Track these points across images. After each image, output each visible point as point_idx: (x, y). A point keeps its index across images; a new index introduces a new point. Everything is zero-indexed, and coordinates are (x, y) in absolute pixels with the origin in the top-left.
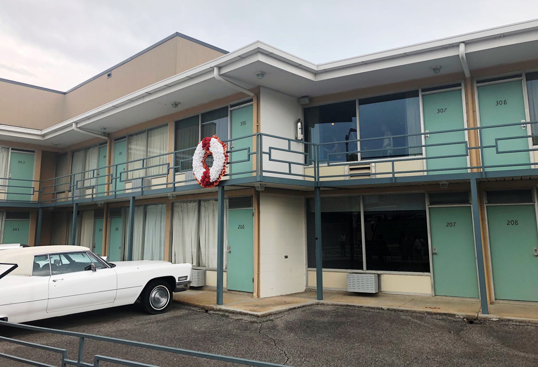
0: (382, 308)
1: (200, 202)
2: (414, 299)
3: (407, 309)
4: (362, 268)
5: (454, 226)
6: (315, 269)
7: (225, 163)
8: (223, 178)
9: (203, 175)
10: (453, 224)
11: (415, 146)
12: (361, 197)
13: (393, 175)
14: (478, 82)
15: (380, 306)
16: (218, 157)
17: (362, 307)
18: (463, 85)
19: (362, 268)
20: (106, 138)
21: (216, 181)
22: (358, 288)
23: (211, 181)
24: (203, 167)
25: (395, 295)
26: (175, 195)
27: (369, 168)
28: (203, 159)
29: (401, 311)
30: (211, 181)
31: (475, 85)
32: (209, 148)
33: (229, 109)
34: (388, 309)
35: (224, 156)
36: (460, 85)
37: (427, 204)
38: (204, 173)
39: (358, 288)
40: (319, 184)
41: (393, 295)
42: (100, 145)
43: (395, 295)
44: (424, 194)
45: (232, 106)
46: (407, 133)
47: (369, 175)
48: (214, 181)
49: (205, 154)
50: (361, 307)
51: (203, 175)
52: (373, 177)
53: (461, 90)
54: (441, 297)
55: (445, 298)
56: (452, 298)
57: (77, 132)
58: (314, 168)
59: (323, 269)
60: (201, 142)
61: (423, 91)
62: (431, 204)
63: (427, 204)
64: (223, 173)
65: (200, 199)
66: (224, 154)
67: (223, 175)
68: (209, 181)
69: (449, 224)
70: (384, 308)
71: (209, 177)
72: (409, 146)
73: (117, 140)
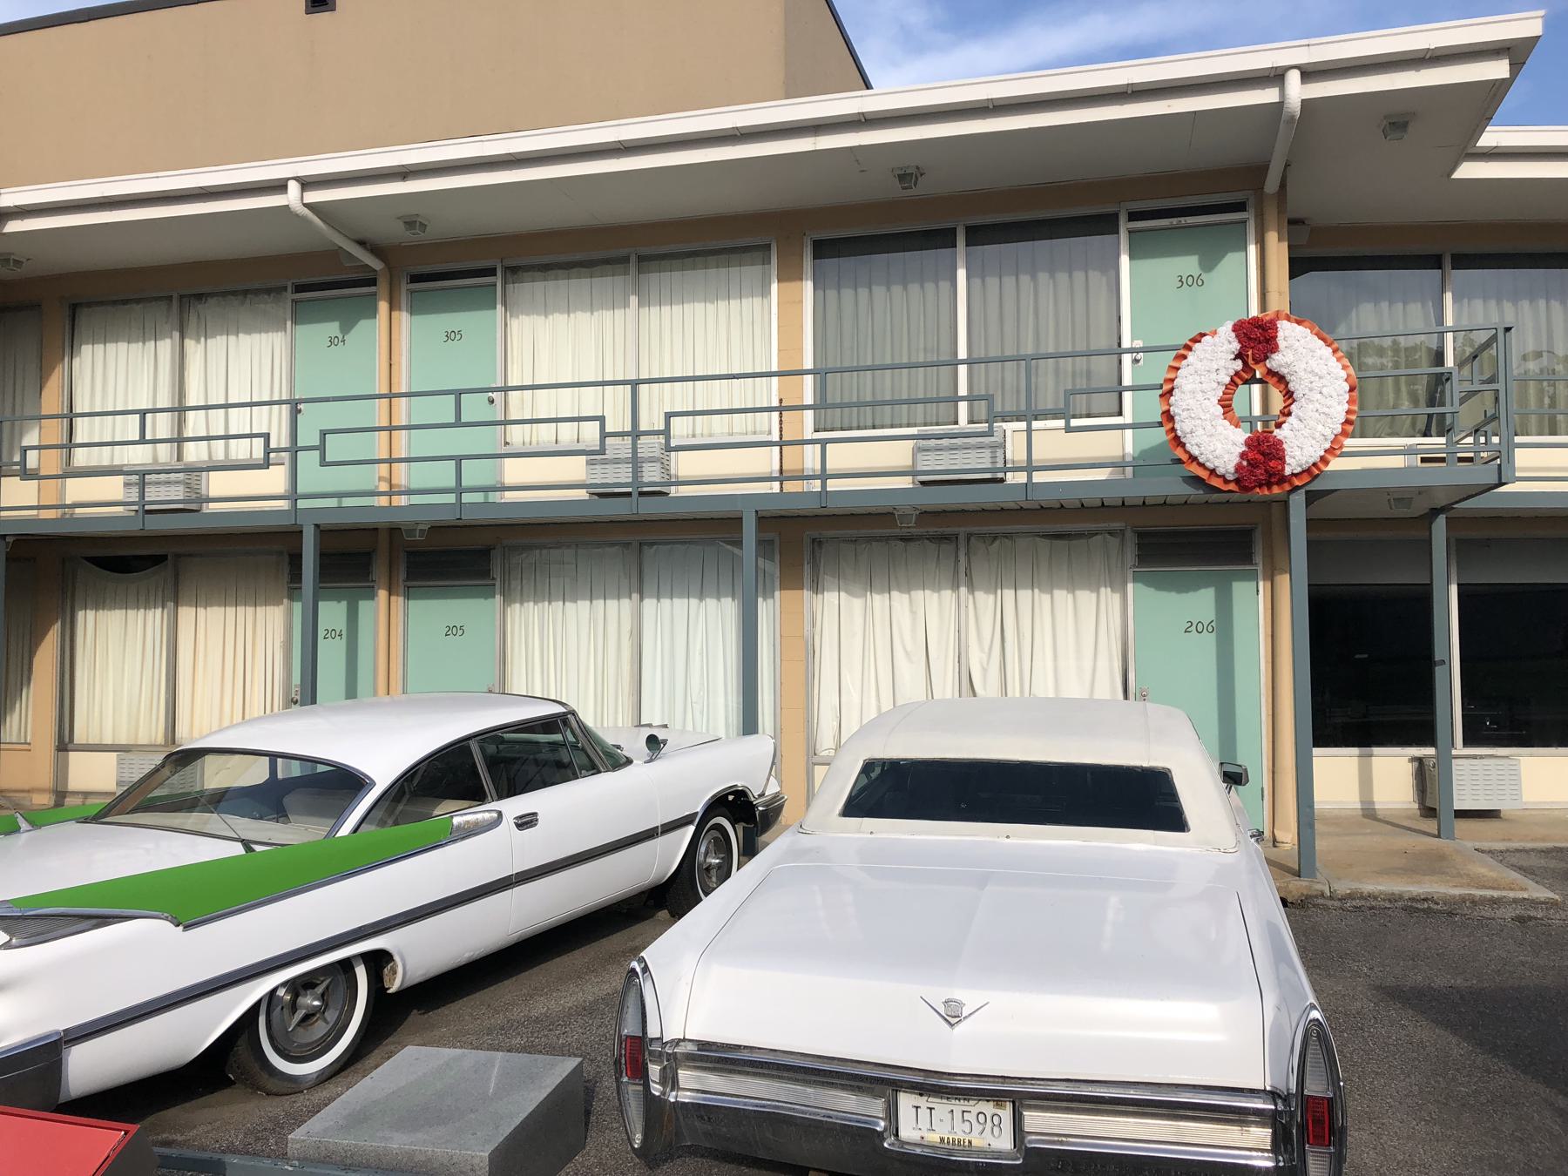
9: (1244, 448)
20: (375, 264)
22: (1487, 797)
23: (1288, 471)
28: (1224, 394)
30: (1288, 471)
32: (1274, 356)
33: (1124, 226)
38: (1248, 443)
39: (1487, 797)
42: (300, 288)
45: (1133, 216)
49: (1237, 374)
51: (1244, 448)
57: (303, 219)
59: (1316, 751)
66: (1346, 380)
68: (1283, 469)
71: (1282, 459)
73: (416, 279)
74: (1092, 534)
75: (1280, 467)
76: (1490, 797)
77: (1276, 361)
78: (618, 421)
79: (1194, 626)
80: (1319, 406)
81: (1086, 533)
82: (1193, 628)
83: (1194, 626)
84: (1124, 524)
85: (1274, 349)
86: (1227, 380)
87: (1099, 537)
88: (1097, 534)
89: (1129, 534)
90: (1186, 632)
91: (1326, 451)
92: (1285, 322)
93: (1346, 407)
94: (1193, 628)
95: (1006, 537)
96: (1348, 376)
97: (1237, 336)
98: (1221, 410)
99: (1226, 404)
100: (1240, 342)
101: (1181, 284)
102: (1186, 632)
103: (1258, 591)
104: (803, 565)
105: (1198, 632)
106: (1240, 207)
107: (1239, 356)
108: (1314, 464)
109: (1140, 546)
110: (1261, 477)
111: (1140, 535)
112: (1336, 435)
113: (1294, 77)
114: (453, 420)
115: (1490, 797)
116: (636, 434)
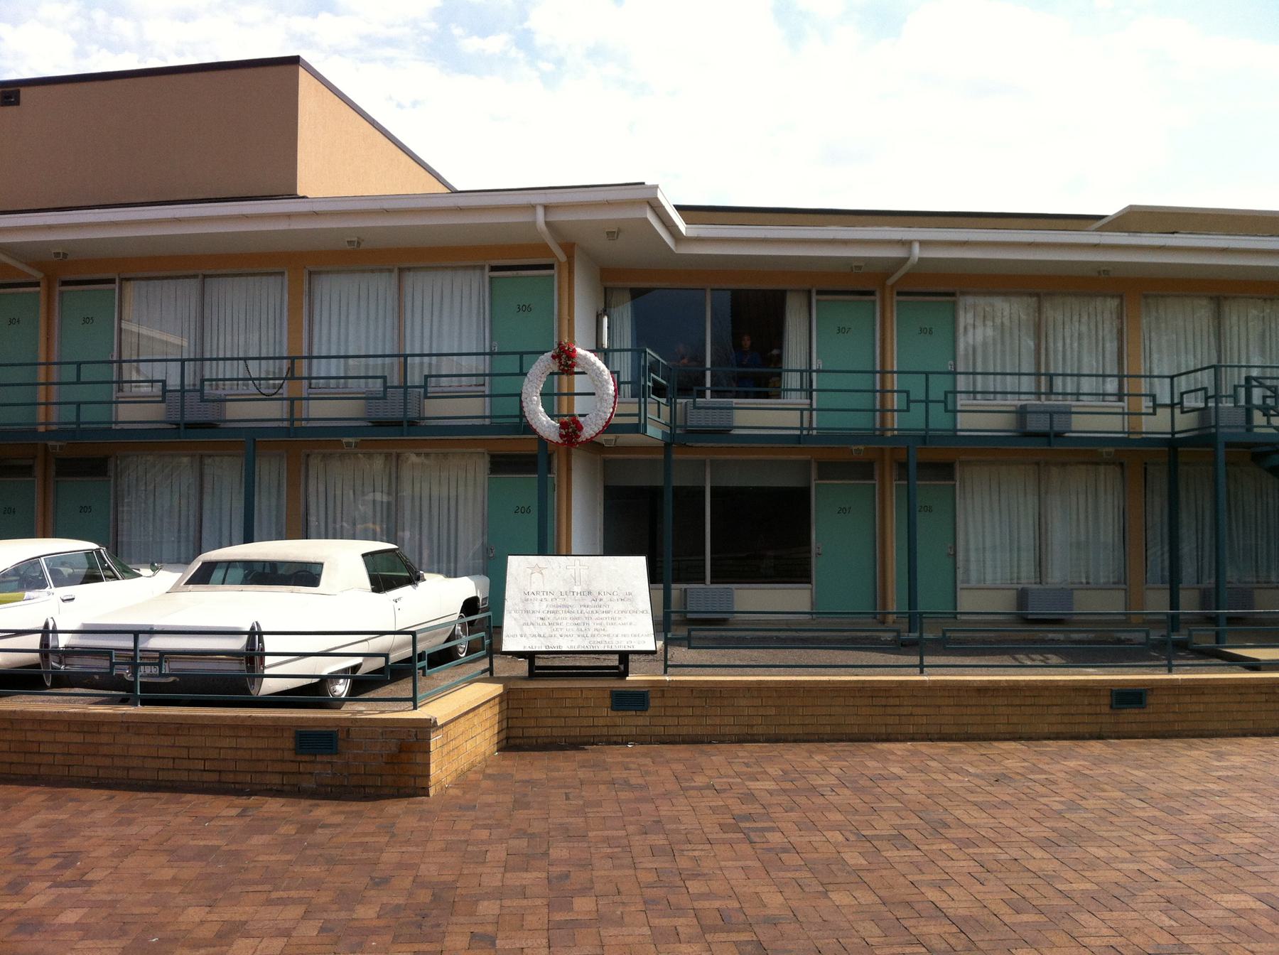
1: (398, 456)
4: (703, 580)
12: (708, 464)
13: (802, 432)
14: (899, 294)
18: (878, 294)
19: (703, 580)
31: (896, 298)
36: (871, 293)
37: (814, 474)
44: (809, 462)
53: (874, 302)
61: (819, 292)
62: (820, 478)
63: (814, 474)
65: (399, 451)
69: (843, 510)
73: (65, 283)
78: (174, 382)
106: (551, 267)
109: (492, 463)
111: (492, 456)
113: (540, 213)
114: (75, 380)
116: (182, 390)
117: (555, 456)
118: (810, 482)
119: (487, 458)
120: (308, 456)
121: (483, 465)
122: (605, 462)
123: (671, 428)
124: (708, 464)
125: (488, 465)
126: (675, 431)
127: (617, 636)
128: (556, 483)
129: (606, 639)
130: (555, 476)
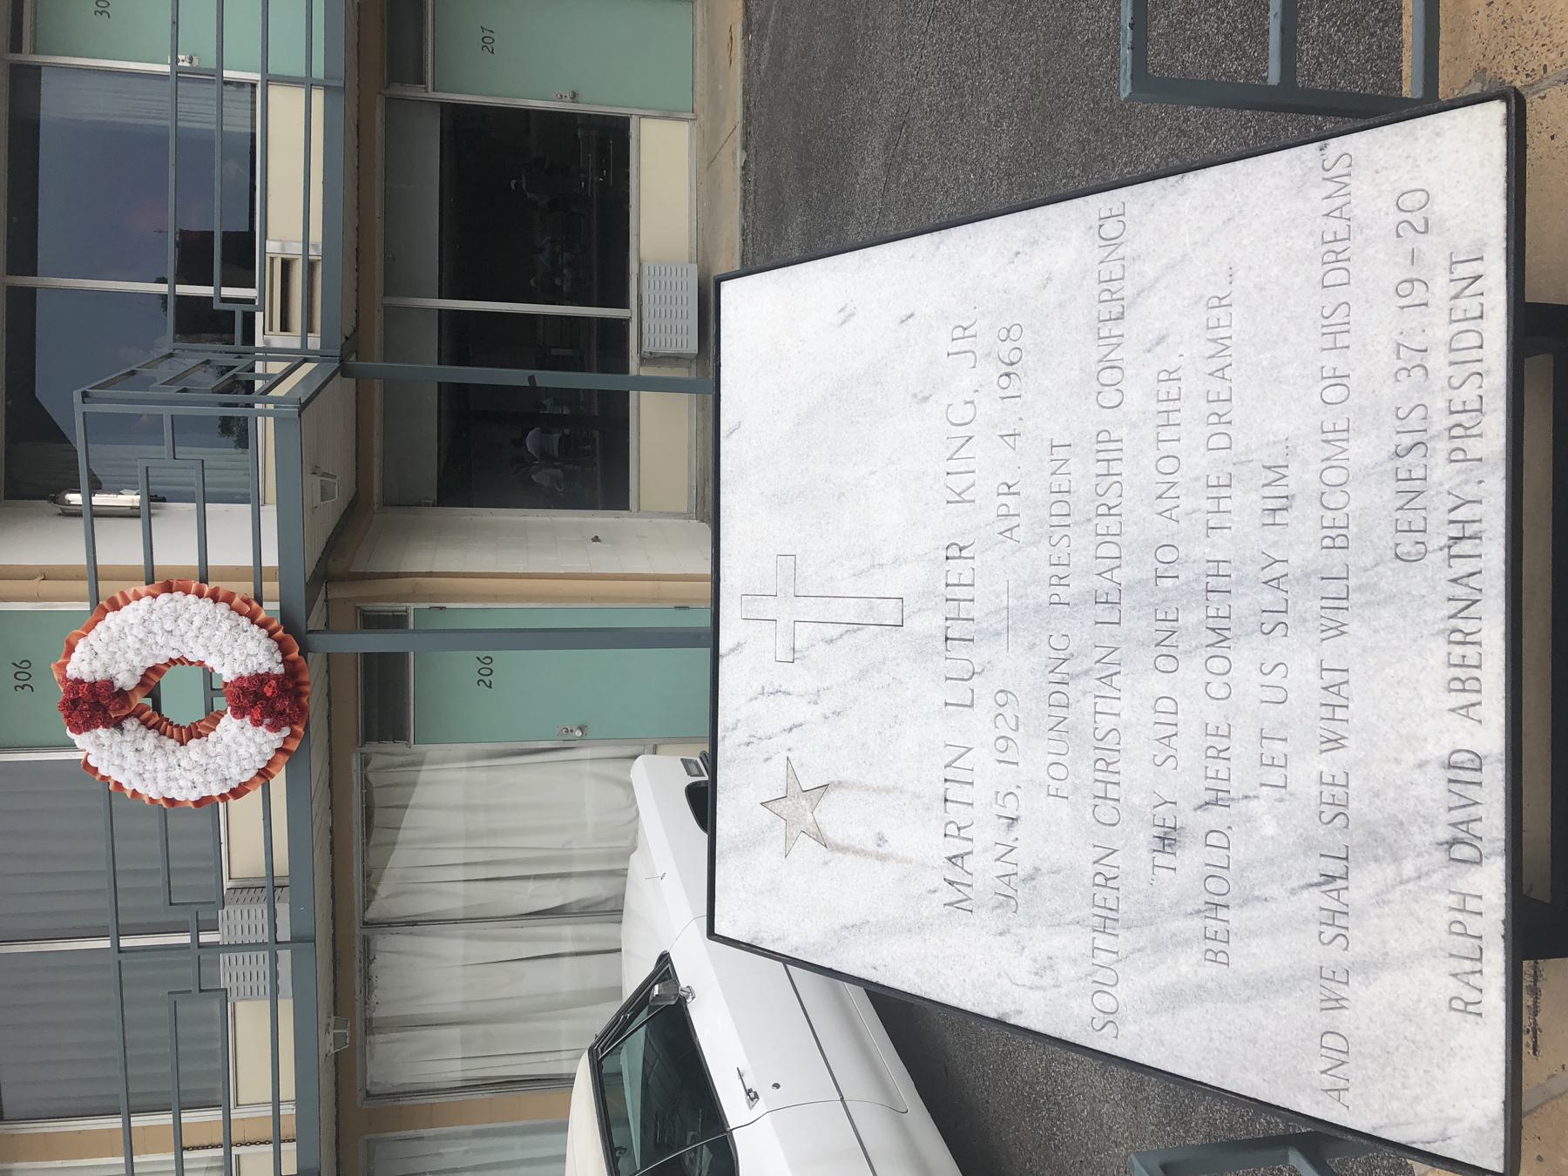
0: (743, 168)
2: (706, 162)
3: (740, 92)
5: (492, 32)
6: (633, 394)
7: (200, 595)
8: (271, 607)
9: (247, 719)
10: (487, 33)
11: (215, 96)
12: (387, 301)
15: (739, 172)
16: (168, 626)
17: (743, 231)
19: (623, 325)
21: (284, 650)
23: (279, 670)
24: (212, 735)
25: (700, 226)
26: (333, 1017)
27: (286, 265)
28: (171, 737)
29: (745, 110)
30: (279, 670)
32: (118, 684)
34: (745, 148)
35: (164, 597)
37: (416, 92)
38: (239, 712)
40: (329, 352)
41: (700, 232)
43: (700, 226)
46: (166, 127)
47: (310, 266)
48: (278, 657)
49: (144, 723)
50: (743, 235)
51: (247, 719)
52: (315, 254)
54: (697, 97)
55: (698, 88)
56: (698, 70)
58: (268, 363)
60: (82, 740)
63: (416, 92)
64: (248, 610)
65: (358, 923)
66: (155, 597)
67: (255, 605)
68: (277, 677)
69: (487, 43)
70: (741, 159)
71: (261, 679)
72: (213, 127)
74: (366, 783)
75: (273, 683)
76: (685, 299)
77: (126, 679)
79: (483, 678)
80: (191, 634)
81: (364, 791)
82: (486, 679)
83: (483, 678)
84: (354, 755)
85: (109, 683)
86: (152, 735)
87: (371, 777)
88: (366, 779)
89: (364, 749)
90: (490, 687)
91: (253, 622)
92: (69, 668)
93: (192, 598)
94: (486, 679)
95: (369, 876)
96: (148, 594)
97: (87, 729)
98: (193, 743)
99: (192, 733)
100: (98, 727)
101: (26, 688)
102: (490, 687)
103: (441, 608)
104: (401, 1107)
105: (491, 673)
107: (118, 725)
108: (271, 635)
109: (382, 738)
110: (287, 703)
111: (368, 737)
112: (232, 609)
115: (685, 299)
117: (368, 606)
118: (433, 103)
119: (373, 747)
120: (368, 1095)
121: (385, 753)
122: (388, 503)
123: (306, 360)
124: (387, 301)
125: (389, 747)
126: (314, 352)
127: (1339, 379)
128: (426, 605)
129: (1367, 449)
130: (412, 606)
